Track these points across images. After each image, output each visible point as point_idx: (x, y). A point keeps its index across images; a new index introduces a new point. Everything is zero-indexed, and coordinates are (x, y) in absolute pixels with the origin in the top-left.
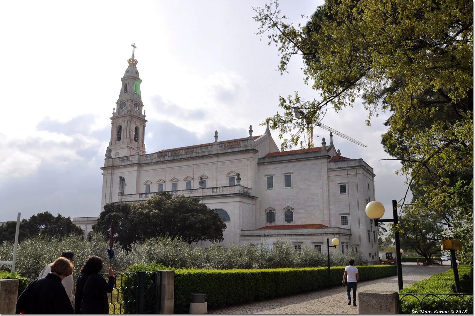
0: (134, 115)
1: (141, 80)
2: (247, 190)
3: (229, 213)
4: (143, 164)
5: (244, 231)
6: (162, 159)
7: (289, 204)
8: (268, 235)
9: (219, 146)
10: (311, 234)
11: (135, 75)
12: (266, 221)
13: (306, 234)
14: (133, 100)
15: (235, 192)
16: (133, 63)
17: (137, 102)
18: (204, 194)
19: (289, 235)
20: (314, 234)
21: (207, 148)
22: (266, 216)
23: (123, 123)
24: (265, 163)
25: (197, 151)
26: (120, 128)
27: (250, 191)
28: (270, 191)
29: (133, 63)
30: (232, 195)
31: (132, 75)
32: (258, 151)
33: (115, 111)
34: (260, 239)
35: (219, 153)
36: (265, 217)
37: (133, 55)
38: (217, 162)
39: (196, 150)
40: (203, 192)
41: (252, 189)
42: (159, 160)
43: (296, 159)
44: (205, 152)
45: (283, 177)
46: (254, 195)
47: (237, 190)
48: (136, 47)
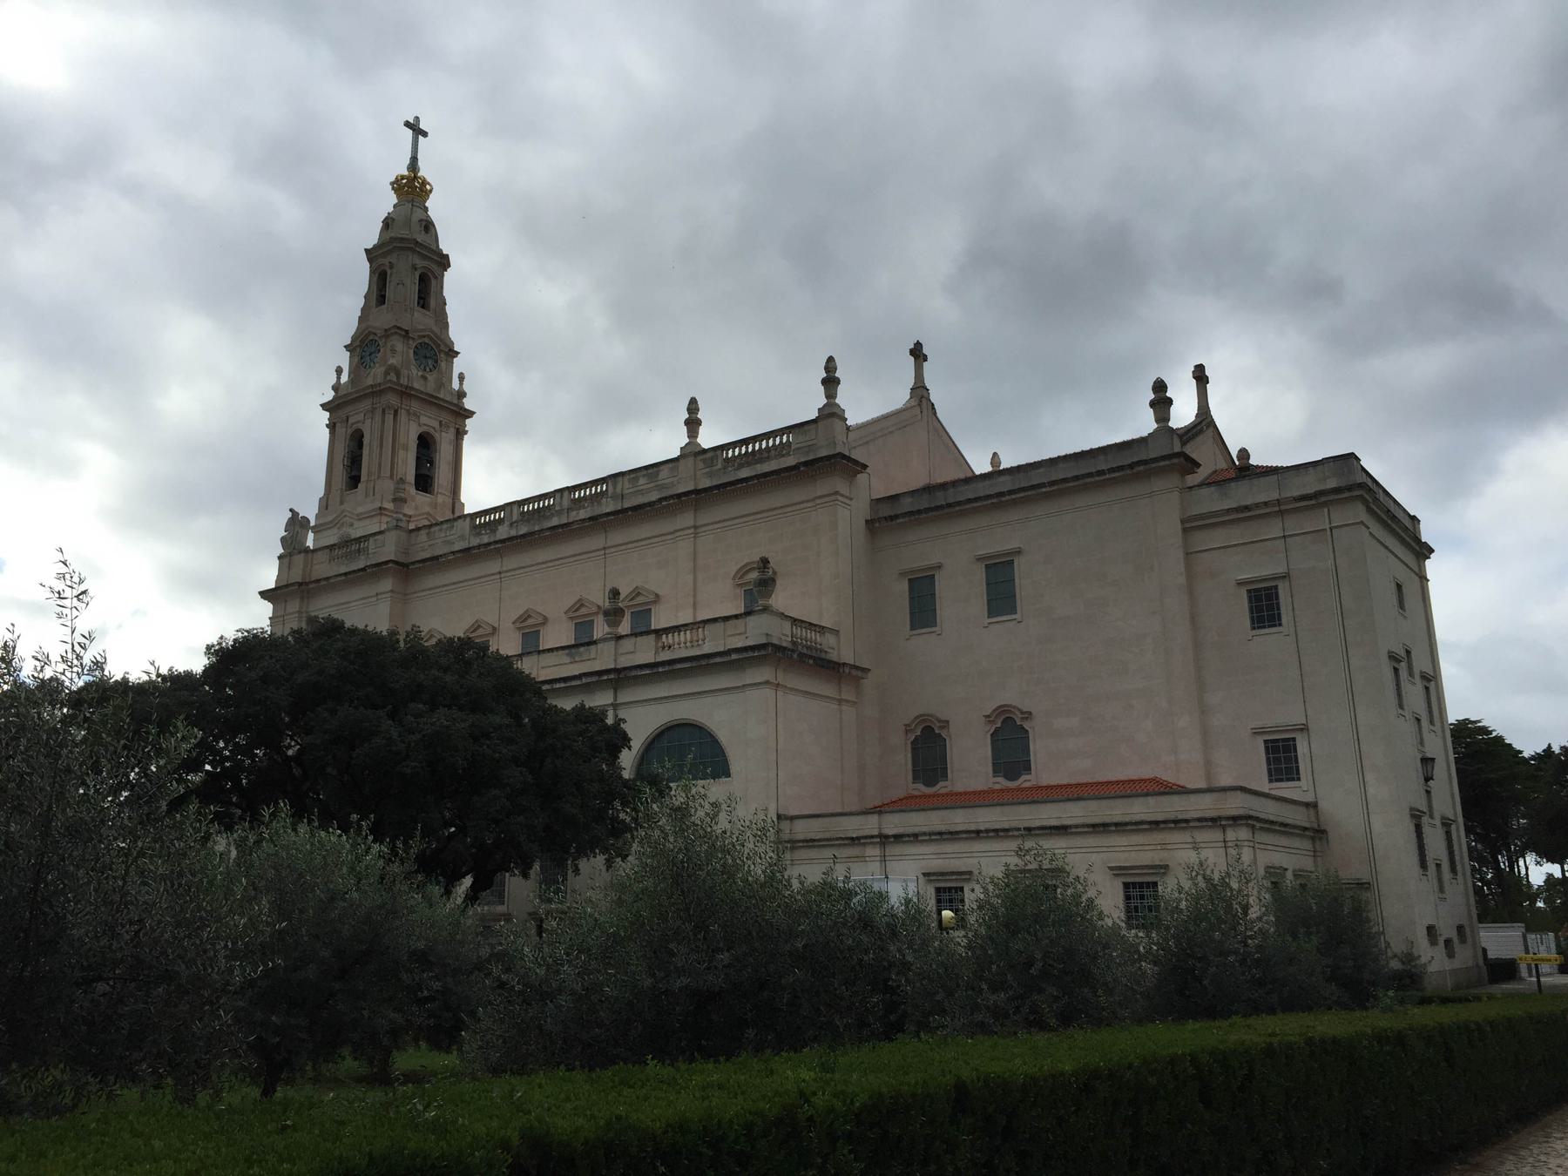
0: (412, 388)
1: (448, 255)
2: (811, 635)
3: (723, 737)
4: (413, 563)
5: (792, 818)
6: (486, 540)
7: (1010, 695)
8: (898, 838)
9: (704, 461)
10: (1104, 825)
11: (421, 238)
12: (910, 777)
13: (1077, 826)
14: (407, 332)
15: (750, 643)
16: (412, 189)
17: (427, 340)
18: (625, 662)
19: (996, 831)
20: (1116, 825)
21: (657, 474)
22: (910, 755)
23: (368, 422)
24: (896, 517)
25: (619, 490)
26: (357, 439)
27: (828, 641)
29: (412, 189)
30: (734, 656)
31: (404, 233)
32: (865, 467)
33: (344, 378)
34: (862, 859)
35: (700, 487)
36: (903, 760)
38: (695, 527)
39: (615, 488)
40: (620, 651)
41: (836, 632)
42: (475, 542)
43: (1033, 487)
44: (649, 491)
45: (980, 575)
46: (847, 657)
47: (754, 631)
48: (425, 134)
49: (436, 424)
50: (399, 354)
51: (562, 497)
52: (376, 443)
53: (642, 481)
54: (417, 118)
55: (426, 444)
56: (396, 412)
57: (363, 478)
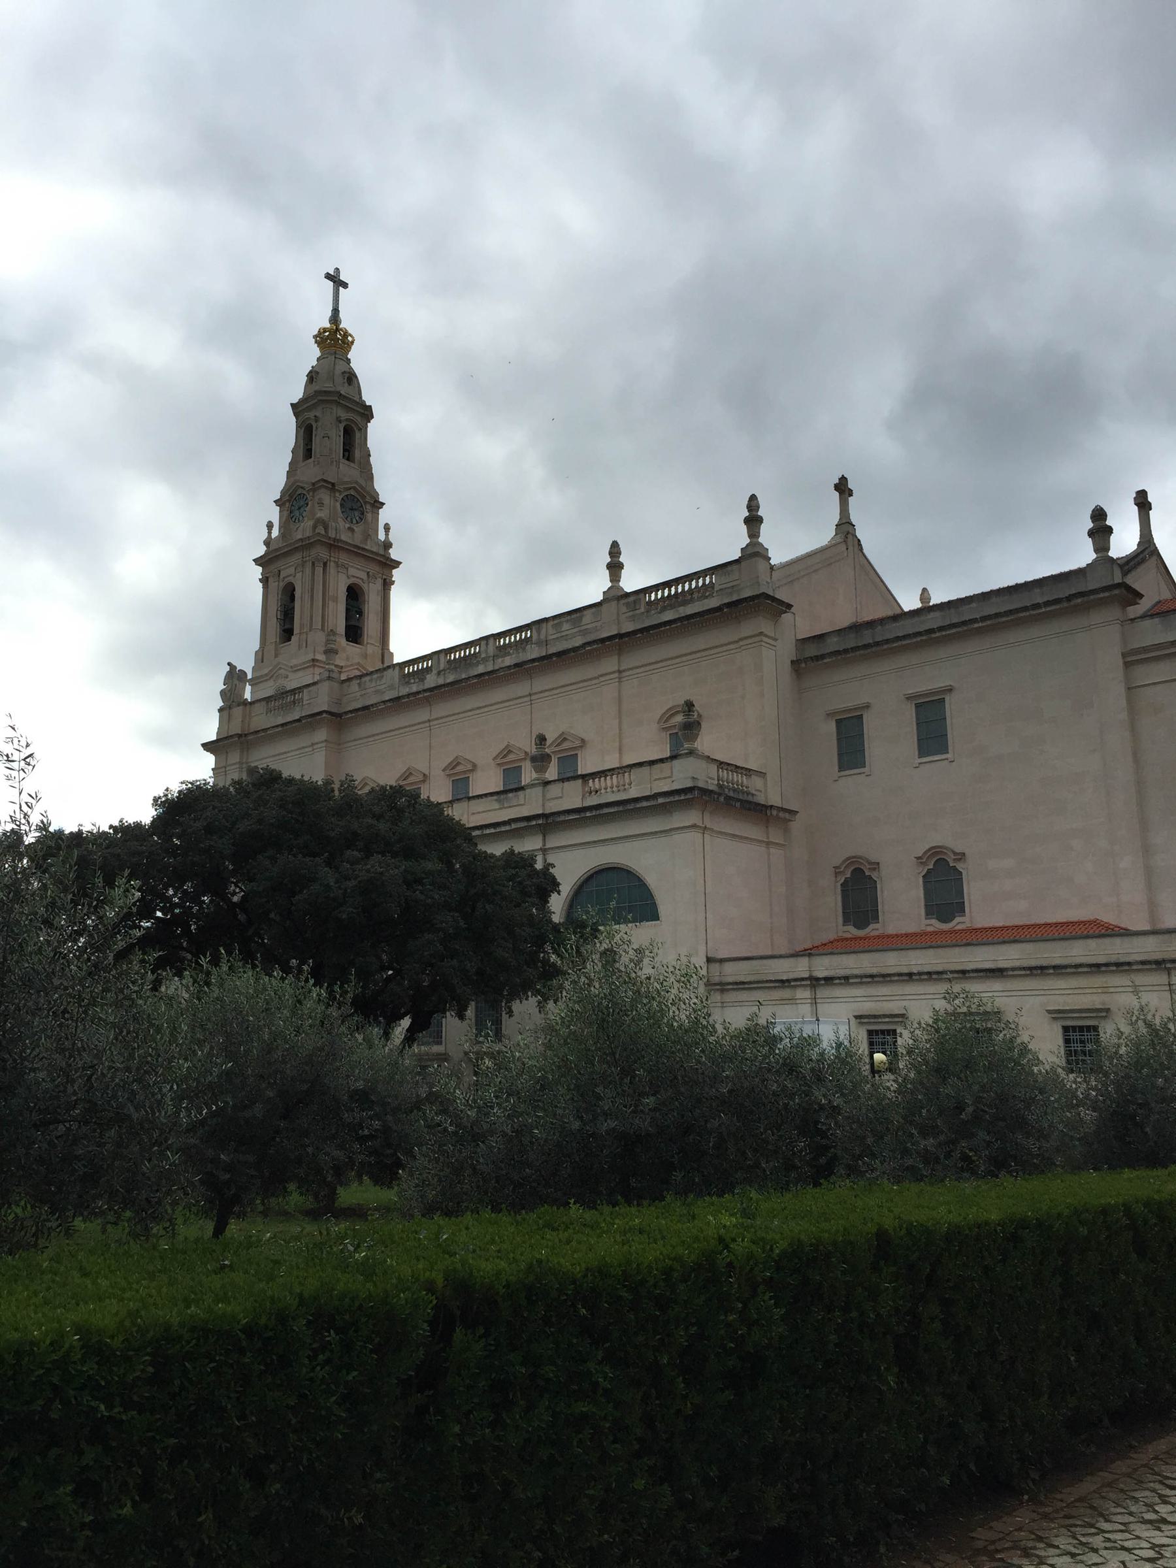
0: (340, 541)
1: (370, 406)
2: (736, 777)
3: (651, 880)
4: (346, 713)
5: (722, 961)
6: (414, 688)
7: (944, 836)
8: (829, 980)
9: (627, 604)
10: (1042, 968)
11: (344, 390)
12: (840, 920)
13: (1013, 969)
14: (333, 484)
15: (677, 786)
17: (352, 492)
18: (553, 807)
19: (929, 973)
20: (1055, 967)
21: (581, 618)
22: (839, 898)
23: (299, 575)
24: (823, 657)
25: (543, 637)
26: (289, 593)
27: (755, 784)
28: (851, 784)
30: (661, 800)
31: (328, 386)
32: (789, 606)
33: (275, 533)
34: (792, 1001)
35: (623, 631)
36: (833, 901)
37: (336, 311)
38: (620, 672)
39: (539, 635)
40: (548, 796)
41: (762, 774)
42: (405, 691)
43: (964, 623)
45: (910, 712)
46: (774, 799)
47: (680, 775)
48: (345, 285)
49: (364, 576)
50: (327, 507)
51: (487, 644)
52: (307, 597)
53: (566, 626)
54: (337, 269)
55: (354, 594)
56: (325, 564)
57: (296, 631)
